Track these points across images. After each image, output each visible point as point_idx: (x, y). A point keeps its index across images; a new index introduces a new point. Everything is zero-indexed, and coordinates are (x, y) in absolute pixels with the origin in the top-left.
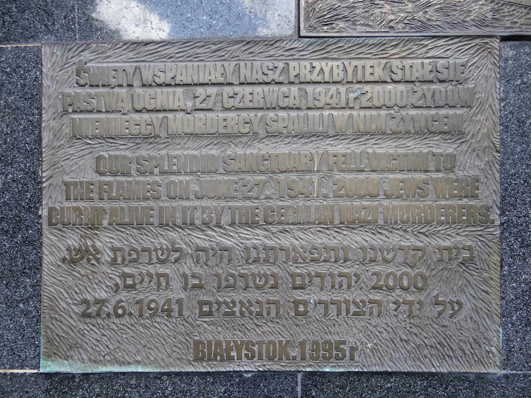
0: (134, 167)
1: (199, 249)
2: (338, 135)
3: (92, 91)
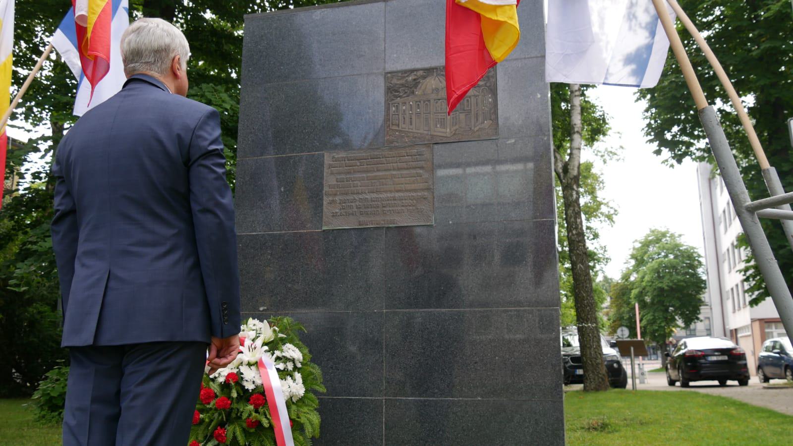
0: (345, 180)
1: (360, 199)
2: (394, 170)
3: (336, 162)
